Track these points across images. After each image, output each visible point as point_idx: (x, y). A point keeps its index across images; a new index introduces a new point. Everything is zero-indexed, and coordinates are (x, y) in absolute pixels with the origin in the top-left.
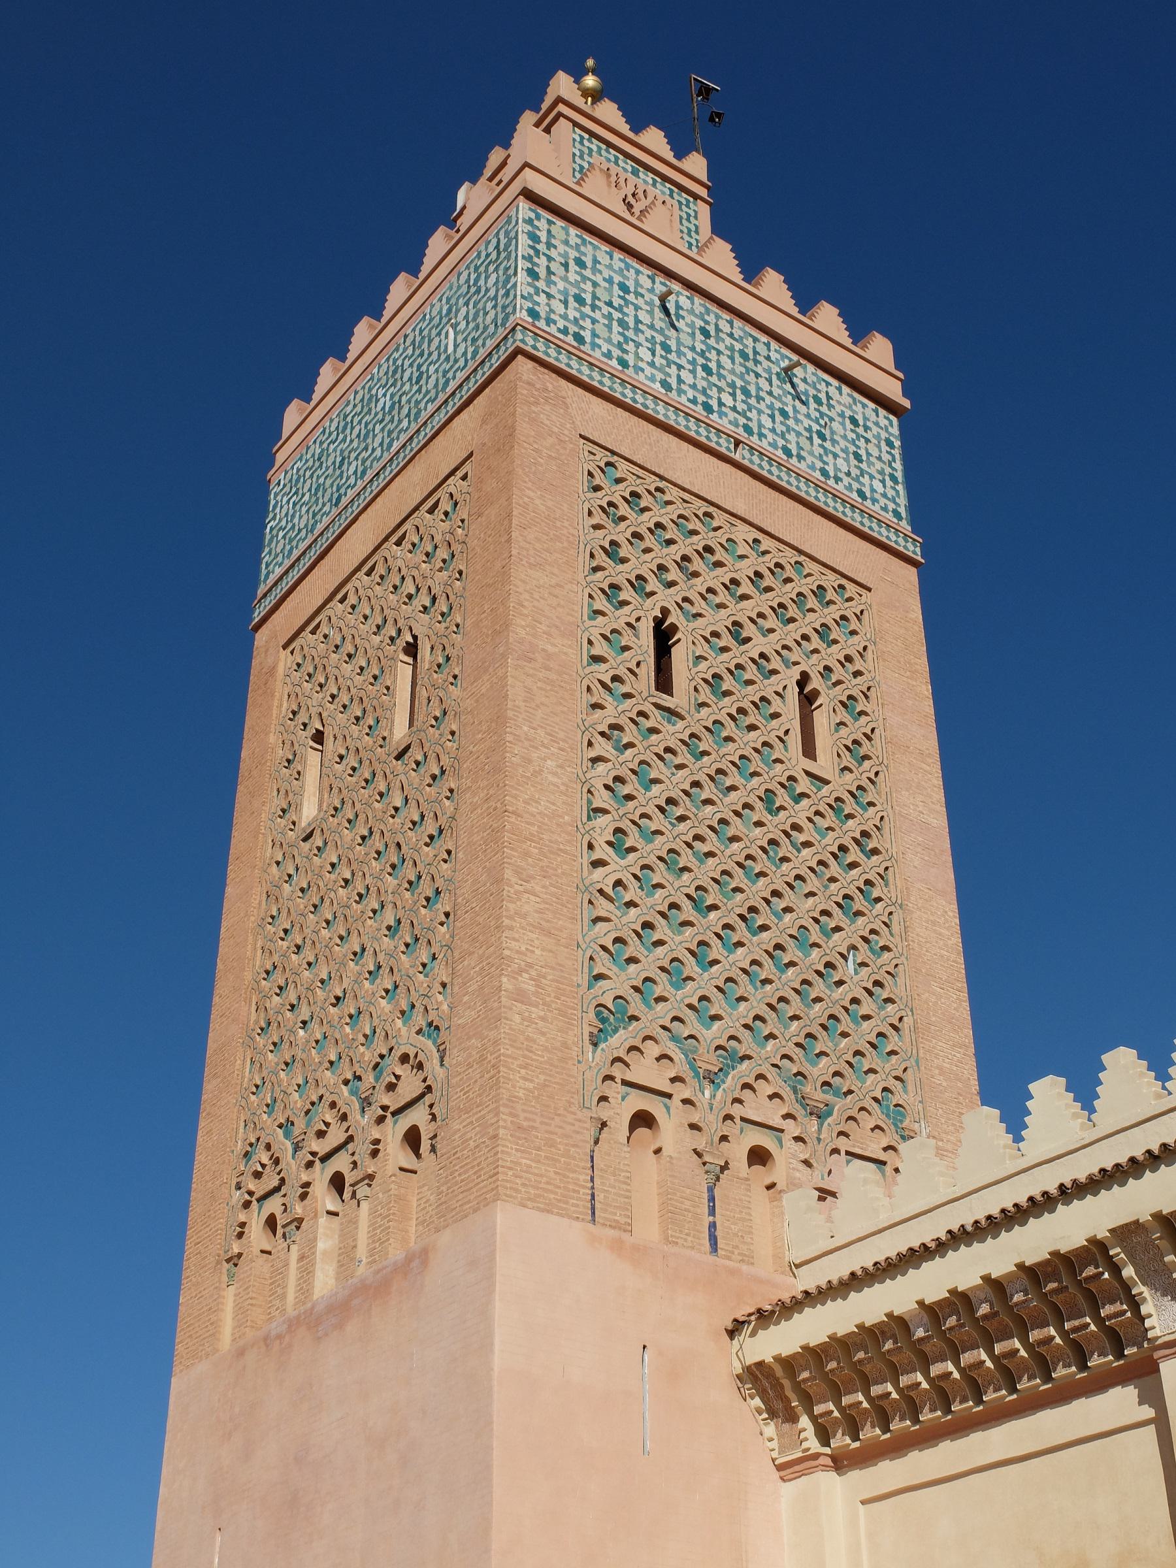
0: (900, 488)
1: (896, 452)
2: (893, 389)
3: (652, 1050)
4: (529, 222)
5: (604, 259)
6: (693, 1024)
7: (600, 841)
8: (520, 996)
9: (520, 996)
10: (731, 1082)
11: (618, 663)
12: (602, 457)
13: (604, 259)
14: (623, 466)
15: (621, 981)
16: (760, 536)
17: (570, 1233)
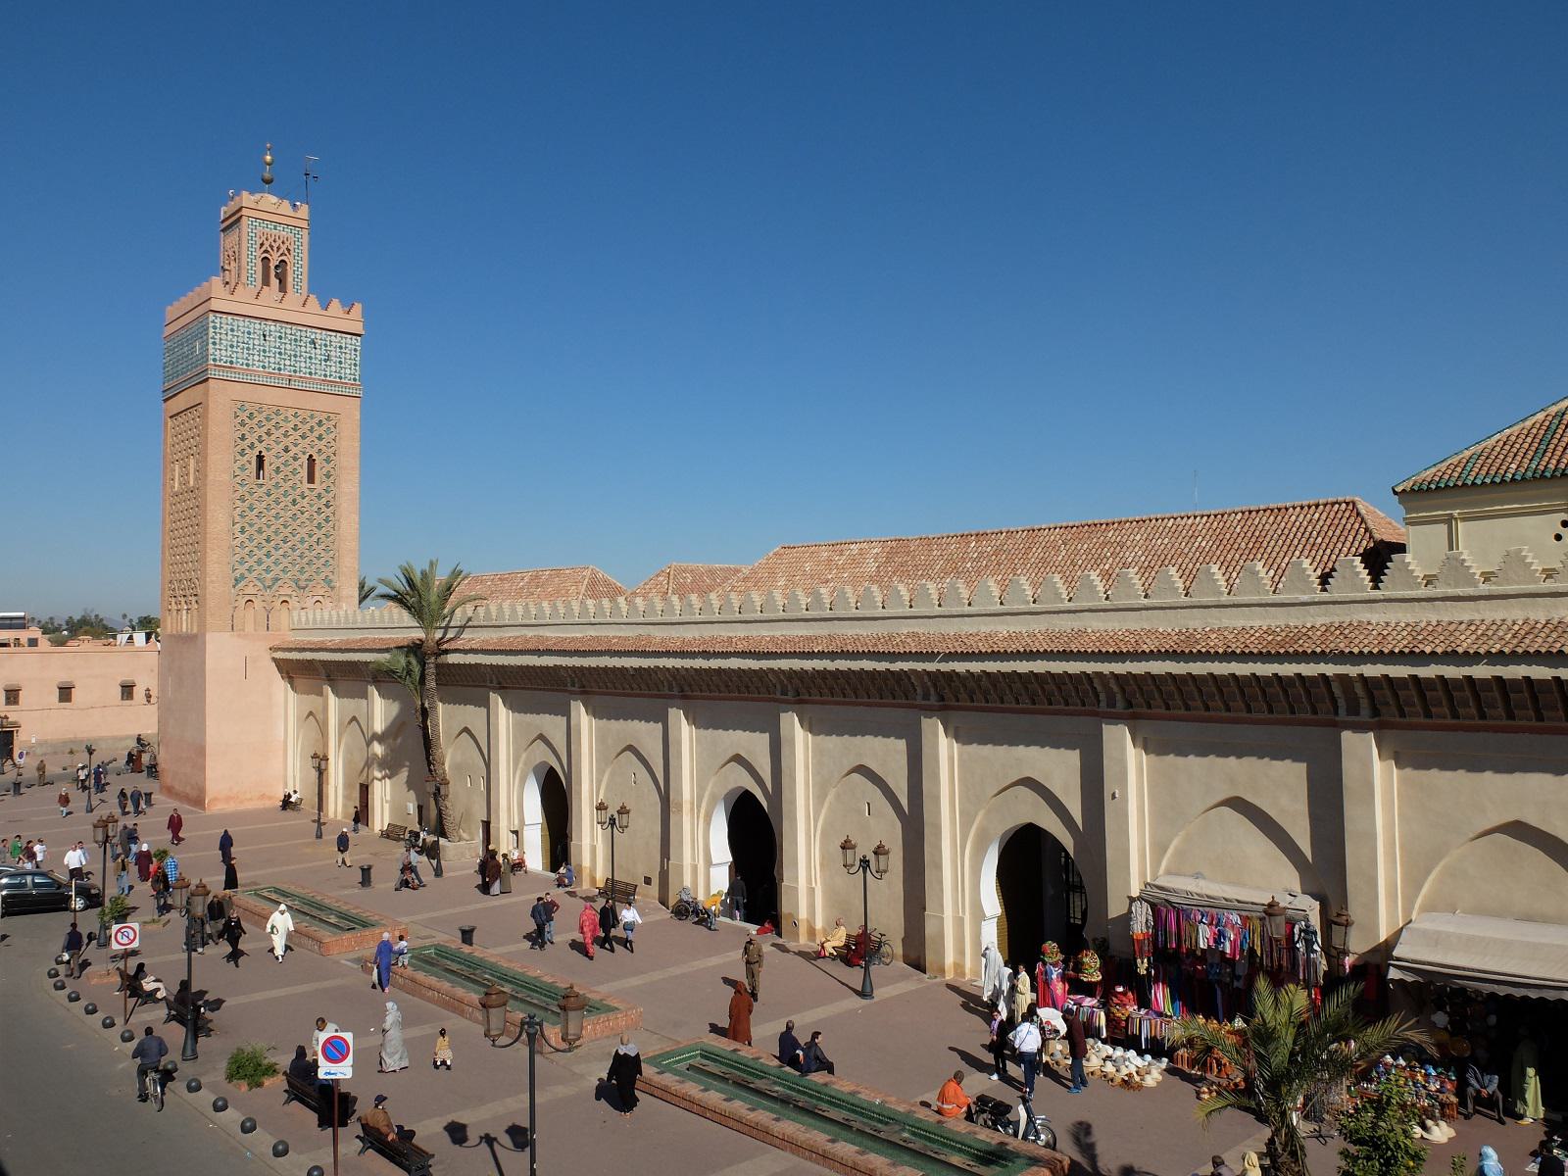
0: (357, 368)
1: (358, 353)
2: (358, 328)
3: (252, 584)
4: (213, 322)
5: (241, 324)
6: (264, 575)
7: (236, 532)
8: (212, 582)
9: (212, 582)
10: (275, 587)
11: (243, 475)
12: (239, 404)
13: (241, 324)
14: (247, 405)
15: (242, 569)
16: (297, 411)
17: (227, 635)
